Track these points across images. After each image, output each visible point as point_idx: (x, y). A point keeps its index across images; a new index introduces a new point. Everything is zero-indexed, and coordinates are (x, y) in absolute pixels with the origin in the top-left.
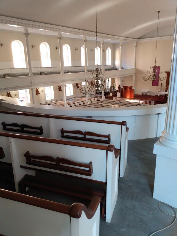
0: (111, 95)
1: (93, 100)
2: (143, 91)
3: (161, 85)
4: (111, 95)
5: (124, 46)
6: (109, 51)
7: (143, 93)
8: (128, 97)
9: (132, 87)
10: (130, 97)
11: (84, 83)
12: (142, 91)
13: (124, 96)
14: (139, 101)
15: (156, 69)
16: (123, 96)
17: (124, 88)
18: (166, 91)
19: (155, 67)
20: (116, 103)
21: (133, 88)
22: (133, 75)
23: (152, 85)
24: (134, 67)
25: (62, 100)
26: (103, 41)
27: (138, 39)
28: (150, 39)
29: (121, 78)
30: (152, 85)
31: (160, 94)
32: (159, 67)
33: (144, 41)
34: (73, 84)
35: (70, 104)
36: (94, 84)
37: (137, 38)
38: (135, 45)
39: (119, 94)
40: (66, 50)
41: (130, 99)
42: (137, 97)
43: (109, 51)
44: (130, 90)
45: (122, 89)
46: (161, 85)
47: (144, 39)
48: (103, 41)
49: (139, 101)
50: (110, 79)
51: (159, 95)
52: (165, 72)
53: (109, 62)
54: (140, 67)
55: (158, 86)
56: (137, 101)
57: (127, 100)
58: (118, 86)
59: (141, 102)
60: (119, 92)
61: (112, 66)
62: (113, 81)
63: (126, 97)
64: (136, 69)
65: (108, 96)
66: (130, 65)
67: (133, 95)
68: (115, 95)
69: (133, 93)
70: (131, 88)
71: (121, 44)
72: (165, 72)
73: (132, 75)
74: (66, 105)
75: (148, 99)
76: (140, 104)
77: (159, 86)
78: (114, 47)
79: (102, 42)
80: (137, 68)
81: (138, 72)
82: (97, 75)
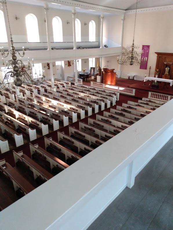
0: (93, 78)
1: (65, 85)
2: (129, 75)
3: (150, 69)
4: (93, 78)
5: (110, 19)
6: (92, 26)
7: (129, 77)
8: (109, 83)
9: (114, 69)
10: (111, 82)
11: (58, 63)
13: (104, 81)
14: (119, 88)
16: (103, 81)
17: (105, 71)
18: (155, 77)
19: (143, 46)
20: (88, 91)
22: (99, 58)
23: (140, 68)
24: (120, 46)
25: (50, 80)
26: (75, 10)
27: (125, 10)
30: (140, 68)
31: (146, 79)
34: (42, 64)
35: (63, 84)
36: (19, 72)
37: (125, 9)
38: (123, 18)
39: (99, 78)
40: (57, 23)
41: (110, 85)
42: (120, 82)
43: (92, 26)
44: (111, 74)
45: (102, 72)
46: (150, 69)
48: (75, 10)
49: (119, 88)
50: (94, 59)
51: (144, 81)
52: (156, 53)
53: (92, 38)
55: (146, 69)
56: (116, 88)
57: (107, 86)
59: (121, 89)
60: (99, 75)
61: (97, 44)
62: (98, 60)
63: (106, 83)
64: (123, 48)
65: (89, 79)
66: (117, 44)
67: (114, 79)
68: (96, 79)
69: (114, 76)
70: (112, 71)
71: (102, 16)
72: (156, 53)
73: (119, 54)
74: (53, 86)
75: (131, 86)
76: (116, 93)
78: (98, 20)
79: (73, 11)
80: (123, 46)
82: (13, 57)
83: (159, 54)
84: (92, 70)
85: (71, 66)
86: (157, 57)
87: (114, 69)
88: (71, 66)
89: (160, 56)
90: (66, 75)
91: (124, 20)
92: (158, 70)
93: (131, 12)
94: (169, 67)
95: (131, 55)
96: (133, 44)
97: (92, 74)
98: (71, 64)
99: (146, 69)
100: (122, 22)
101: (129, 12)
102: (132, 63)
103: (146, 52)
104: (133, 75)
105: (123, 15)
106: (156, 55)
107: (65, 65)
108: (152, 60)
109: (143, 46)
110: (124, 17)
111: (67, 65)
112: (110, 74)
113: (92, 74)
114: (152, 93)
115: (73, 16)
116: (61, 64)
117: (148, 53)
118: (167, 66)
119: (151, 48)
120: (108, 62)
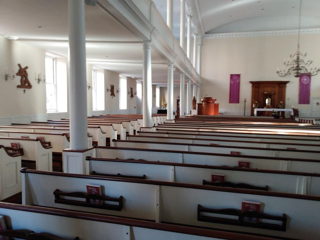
9: (216, 100)
15: (235, 79)
19: (232, 76)
21: (216, 102)
23: (230, 102)
30: (230, 102)
32: (239, 76)
33: (214, 37)
46: (245, 102)
47: (215, 35)
52: (251, 82)
54: (209, 75)
55: (238, 102)
64: (201, 78)
77: (241, 105)
80: (202, 76)
87: (216, 100)
89: (256, 85)
92: (256, 102)
93: (213, 36)
94: (270, 98)
99: (238, 102)
105: (200, 40)
106: (251, 85)
108: (246, 91)
109: (232, 76)
110: (202, 42)
117: (239, 83)
118: (269, 96)
119: (241, 77)
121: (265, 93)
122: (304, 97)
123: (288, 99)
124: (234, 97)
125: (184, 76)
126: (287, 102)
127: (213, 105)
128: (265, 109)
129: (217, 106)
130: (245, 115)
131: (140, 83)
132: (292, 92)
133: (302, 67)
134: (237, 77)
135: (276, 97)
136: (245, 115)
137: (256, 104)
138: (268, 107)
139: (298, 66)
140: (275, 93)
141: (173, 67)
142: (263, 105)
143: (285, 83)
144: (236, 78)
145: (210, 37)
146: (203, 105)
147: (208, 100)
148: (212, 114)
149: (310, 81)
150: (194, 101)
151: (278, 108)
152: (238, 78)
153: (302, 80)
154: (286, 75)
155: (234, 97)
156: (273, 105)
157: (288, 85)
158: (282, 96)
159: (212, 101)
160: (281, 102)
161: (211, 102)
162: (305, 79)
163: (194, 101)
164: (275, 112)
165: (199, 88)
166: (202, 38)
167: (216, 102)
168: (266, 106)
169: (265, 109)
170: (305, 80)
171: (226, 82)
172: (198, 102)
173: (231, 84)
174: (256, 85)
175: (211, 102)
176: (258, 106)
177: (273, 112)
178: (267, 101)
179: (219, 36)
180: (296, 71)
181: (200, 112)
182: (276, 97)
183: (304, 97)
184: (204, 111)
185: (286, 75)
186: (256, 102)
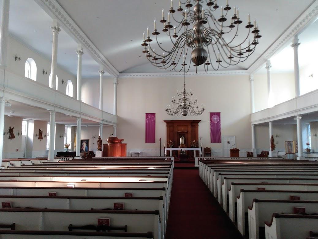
3: (160, 141)
9: (123, 140)
12: (130, 152)
15: (150, 118)
19: (147, 115)
21: (123, 142)
23: (146, 142)
27: (120, 73)
28: (138, 74)
29: (102, 125)
30: (146, 142)
32: (154, 115)
33: (129, 76)
38: (115, 81)
45: (106, 145)
46: (160, 141)
47: (129, 74)
52: (165, 121)
54: (125, 114)
55: (154, 142)
58: (98, 139)
73: (114, 125)
80: (118, 115)
81: (121, 122)
83: (167, 122)
84: (85, 144)
85: (42, 138)
86: (166, 127)
87: (123, 140)
88: (42, 138)
89: (170, 124)
90: (36, 154)
91: (117, 84)
92: (171, 141)
93: (127, 76)
95: (183, 104)
96: (185, 90)
97: (84, 150)
98: (43, 136)
99: (154, 142)
100: (115, 86)
101: (124, 76)
102: (186, 113)
103: (152, 122)
104: (138, 151)
105: (116, 79)
106: (165, 124)
107: (35, 135)
108: (161, 131)
109: (147, 115)
110: (117, 81)
111: (38, 137)
112: (118, 145)
113: (84, 150)
114: (199, 159)
115: (78, 55)
116: (26, 135)
117: (154, 122)
118: (181, 135)
120: (94, 137)
121: (179, 132)
122: (216, 136)
123: (201, 138)
124: (150, 136)
125: (54, 114)
126: (200, 141)
127: (118, 145)
128: (179, 149)
129: (123, 147)
130: (160, 156)
131: (32, 122)
132: (204, 131)
133: (189, 106)
134: (153, 116)
135: (189, 136)
136: (160, 156)
137: (171, 143)
138: (182, 147)
139: (185, 105)
140: (188, 132)
141: (4, 102)
142: (177, 145)
143: (198, 122)
144: (151, 118)
145: (124, 77)
146: (109, 145)
147: (113, 140)
148: (118, 155)
149: (220, 120)
150: (100, 141)
151: (192, 147)
152: (154, 117)
153: (212, 119)
154: (175, 113)
155: (150, 136)
156: (187, 145)
157: (200, 124)
158: (195, 135)
159: (117, 141)
160: (194, 141)
161: (117, 142)
162: (215, 118)
163: (100, 141)
164: (183, 152)
165: (116, 128)
166: (118, 77)
167: (123, 142)
168: (180, 146)
169: (179, 149)
170: (215, 119)
171: (142, 122)
172: (104, 142)
173: (146, 123)
174: (170, 124)
175: (117, 142)
176: (172, 146)
177: (181, 151)
178: (181, 140)
179: (134, 76)
180: (182, 110)
181: (105, 154)
182: (189, 136)
183: (216, 136)
184: (109, 153)
185: (175, 113)
186: (171, 141)
